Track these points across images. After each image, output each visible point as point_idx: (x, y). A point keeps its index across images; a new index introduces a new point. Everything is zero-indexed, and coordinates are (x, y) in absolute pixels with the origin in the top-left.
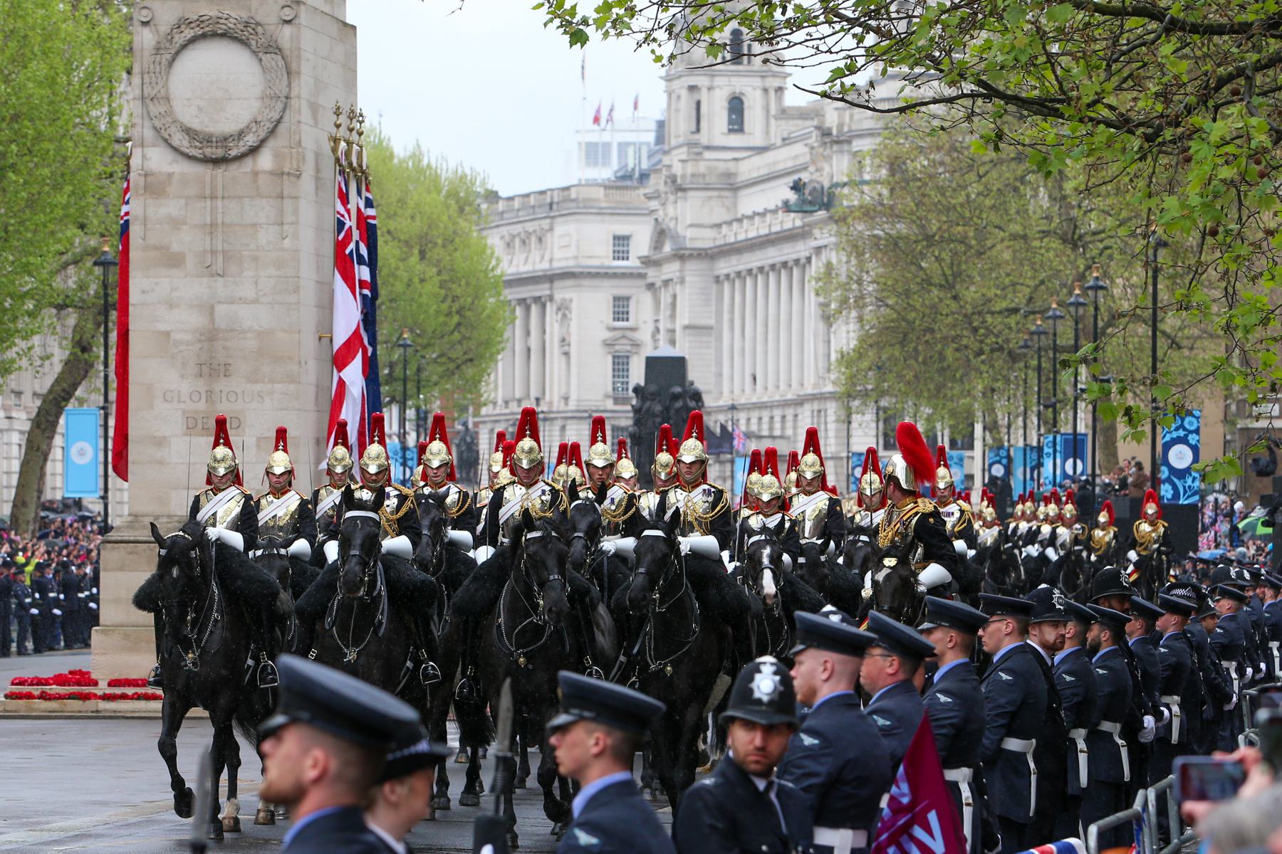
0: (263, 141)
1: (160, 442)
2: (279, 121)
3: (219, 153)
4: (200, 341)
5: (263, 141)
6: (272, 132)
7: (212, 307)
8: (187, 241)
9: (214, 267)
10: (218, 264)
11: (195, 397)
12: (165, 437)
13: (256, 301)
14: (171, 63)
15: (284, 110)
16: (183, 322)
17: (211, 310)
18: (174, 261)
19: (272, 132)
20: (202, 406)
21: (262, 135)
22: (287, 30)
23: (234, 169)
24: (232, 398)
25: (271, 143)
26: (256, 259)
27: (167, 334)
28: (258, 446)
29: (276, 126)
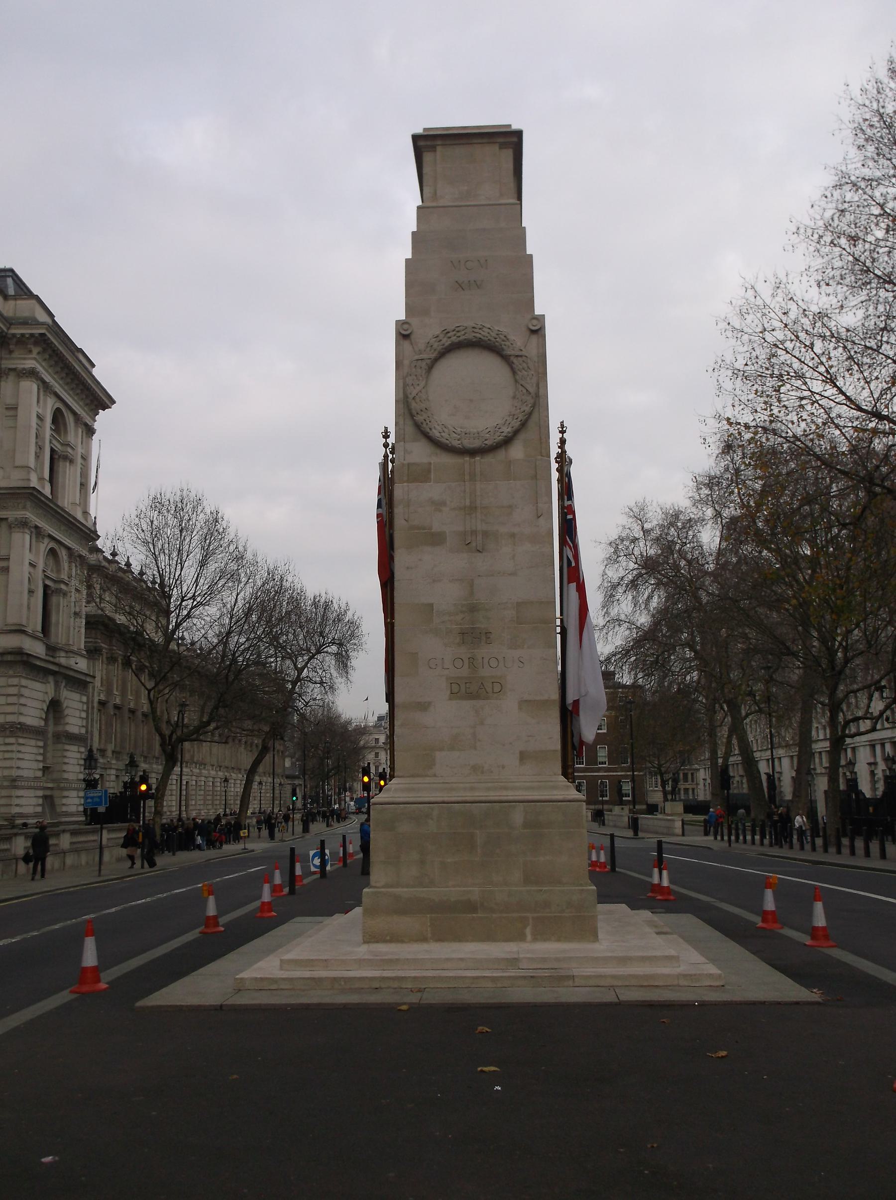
0: (516, 432)
1: (424, 707)
2: (530, 414)
3: (476, 444)
4: (462, 612)
5: (516, 432)
6: (524, 424)
7: (472, 580)
8: (446, 522)
9: (474, 544)
10: (474, 543)
11: (459, 663)
12: (430, 703)
13: (514, 574)
14: (430, 368)
15: (534, 406)
16: (446, 596)
17: (471, 585)
18: (435, 539)
19: (524, 424)
20: (465, 672)
21: (516, 424)
22: (534, 339)
23: (489, 459)
24: (493, 663)
25: (522, 436)
26: (513, 536)
27: (431, 605)
28: (520, 709)
29: (526, 420)
